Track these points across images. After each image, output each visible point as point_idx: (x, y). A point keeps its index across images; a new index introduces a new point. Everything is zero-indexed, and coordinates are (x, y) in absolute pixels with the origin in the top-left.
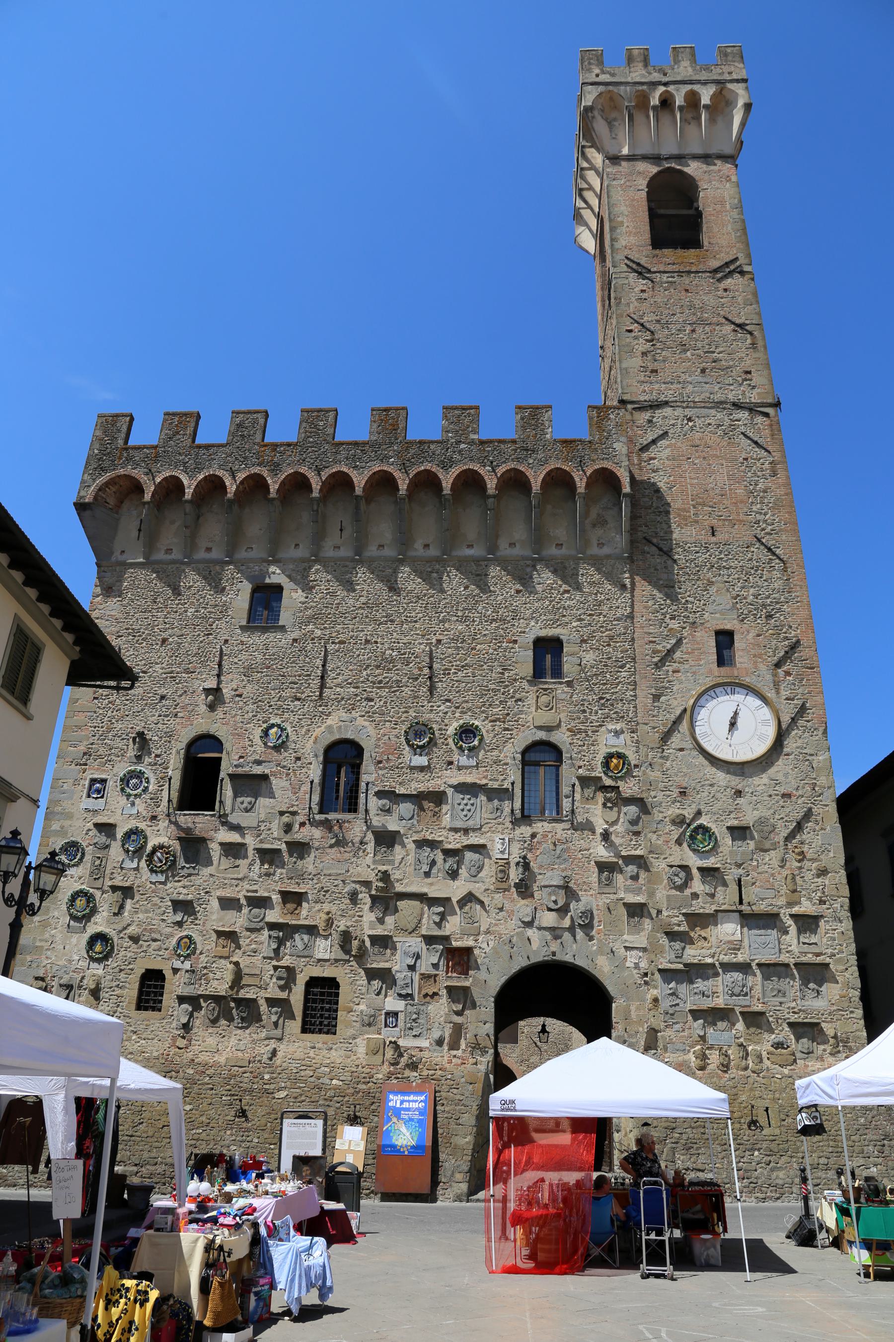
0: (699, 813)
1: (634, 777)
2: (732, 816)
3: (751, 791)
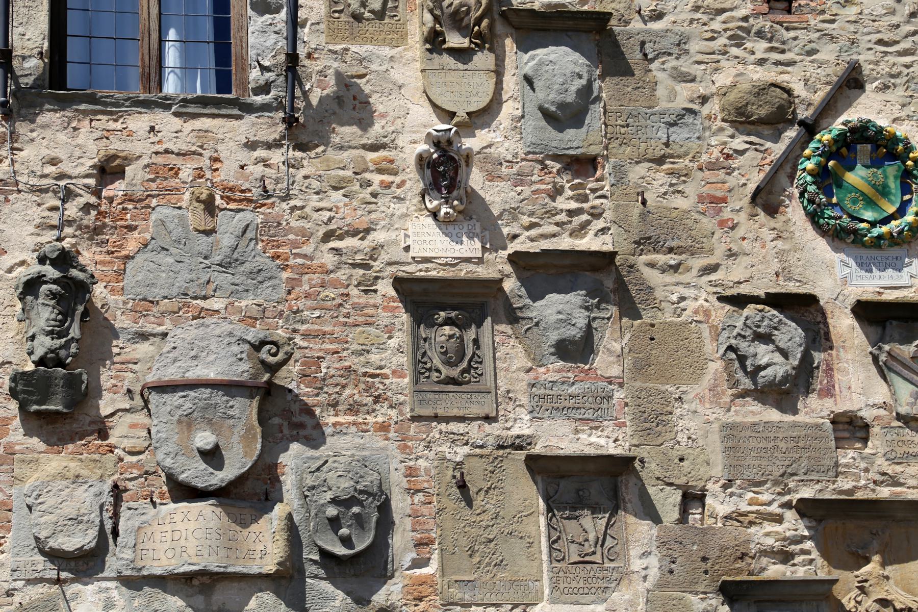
0: (852, 82)
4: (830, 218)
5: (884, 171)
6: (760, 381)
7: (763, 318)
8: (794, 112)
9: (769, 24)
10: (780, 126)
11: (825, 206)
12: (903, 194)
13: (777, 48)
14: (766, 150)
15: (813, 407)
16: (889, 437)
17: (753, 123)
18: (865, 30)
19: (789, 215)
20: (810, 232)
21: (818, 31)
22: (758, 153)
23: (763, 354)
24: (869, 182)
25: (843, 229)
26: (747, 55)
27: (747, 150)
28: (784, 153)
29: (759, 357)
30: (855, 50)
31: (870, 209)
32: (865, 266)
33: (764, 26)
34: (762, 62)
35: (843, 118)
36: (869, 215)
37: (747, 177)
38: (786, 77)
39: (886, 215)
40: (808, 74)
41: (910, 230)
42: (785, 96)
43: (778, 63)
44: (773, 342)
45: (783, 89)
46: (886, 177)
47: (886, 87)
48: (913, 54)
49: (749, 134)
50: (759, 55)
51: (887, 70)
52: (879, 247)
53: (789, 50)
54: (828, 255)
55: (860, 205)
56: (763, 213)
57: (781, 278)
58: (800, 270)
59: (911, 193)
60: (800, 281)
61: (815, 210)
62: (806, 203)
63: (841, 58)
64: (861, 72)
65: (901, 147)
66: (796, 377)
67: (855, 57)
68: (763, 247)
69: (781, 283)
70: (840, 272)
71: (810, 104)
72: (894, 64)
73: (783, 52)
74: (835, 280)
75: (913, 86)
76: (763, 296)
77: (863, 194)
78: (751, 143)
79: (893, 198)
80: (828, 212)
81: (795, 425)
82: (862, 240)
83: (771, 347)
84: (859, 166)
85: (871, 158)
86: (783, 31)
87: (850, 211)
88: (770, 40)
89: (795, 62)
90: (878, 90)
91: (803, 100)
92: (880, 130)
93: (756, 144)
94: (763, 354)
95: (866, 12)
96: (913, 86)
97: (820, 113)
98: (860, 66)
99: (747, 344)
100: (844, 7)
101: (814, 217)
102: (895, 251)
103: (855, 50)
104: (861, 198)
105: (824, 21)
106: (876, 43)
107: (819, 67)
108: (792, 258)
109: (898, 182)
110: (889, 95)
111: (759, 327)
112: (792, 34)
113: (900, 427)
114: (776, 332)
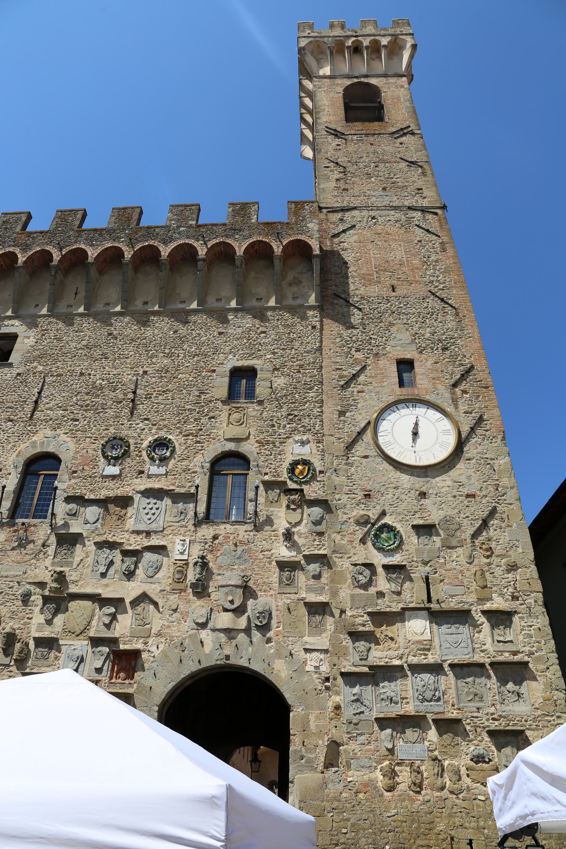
1: (318, 481)
2: (417, 515)
3: (435, 492)
34: (363, 510)
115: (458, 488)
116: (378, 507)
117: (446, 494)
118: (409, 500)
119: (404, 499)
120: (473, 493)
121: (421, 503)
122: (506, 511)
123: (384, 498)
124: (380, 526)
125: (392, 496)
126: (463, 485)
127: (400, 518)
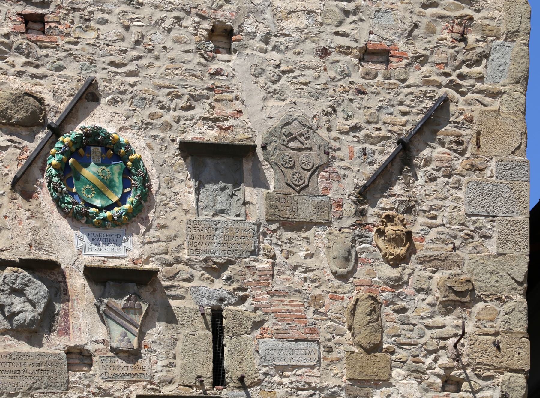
0: (89, 95)
2: (200, 111)
3: (263, 30)
4: (69, 203)
5: (112, 168)
6: (15, 323)
7: (17, 277)
8: (45, 118)
9: (26, 42)
10: (35, 128)
11: (66, 193)
12: (124, 187)
13: (33, 63)
14: (23, 147)
15: (54, 342)
16: (104, 363)
17: (12, 125)
18: (101, 53)
19: (40, 200)
20: (56, 214)
21: (65, 50)
22: (17, 150)
23: (18, 303)
24: (99, 177)
25: (78, 212)
26: (8, 67)
27: (8, 147)
28: (36, 150)
29: (14, 306)
30: (93, 69)
31: (99, 198)
32: (95, 241)
33: (22, 43)
34: (20, 74)
35: (83, 124)
36: (98, 202)
37: (9, 168)
38: (38, 88)
39: (111, 202)
40: (56, 87)
41: (127, 214)
42: (37, 104)
43: (33, 76)
44: (25, 295)
45: (35, 98)
46: (112, 174)
47: (115, 102)
48: (136, 75)
49: (10, 134)
50: (18, 68)
51: (117, 87)
52: (105, 227)
53: (42, 65)
54: (68, 232)
55: (93, 194)
56: (20, 198)
57: (33, 248)
58: (48, 242)
59: (131, 187)
60: (47, 251)
61: (58, 196)
62: (52, 190)
63: (82, 75)
64: (97, 88)
65: (123, 150)
66: (42, 320)
67: (93, 75)
68: (20, 224)
69: (34, 251)
70: (77, 245)
71: (57, 112)
72: (122, 83)
73: (37, 66)
74: (73, 251)
75: (136, 102)
76: (18, 261)
77: (94, 186)
78: (11, 141)
79: (117, 190)
80: (68, 199)
81: (40, 355)
82: (92, 221)
83: (23, 299)
84: (92, 164)
85: (102, 158)
86: (38, 49)
87: (85, 198)
88: (28, 56)
89: (47, 76)
90: (110, 103)
91: (52, 108)
92: (108, 136)
93: (16, 142)
94: (18, 303)
95: (102, 37)
96: (136, 102)
97: (64, 119)
98: (96, 83)
99: (5, 296)
100: (85, 31)
101: (58, 202)
102: (117, 231)
103: (93, 69)
104: (93, 189)
105: (69, 43)
106: (109, 64)
107: (65, 81)
108: (42, 233)
109: (121, 177)
110: (118, 109)
111: (14, 284)
112: (44, 52)
113: (112, 356)
114: (27, 288)
115: (340, 23)
116: (72, 70)
117: (298, 42)
118: (176, 52)
119: (159, 47)
120: (386, 45)
121: (214, 67)
122: (476, 115)
123: (91, 36)
124: (79, 138)
125: (121, 30)
126: (355, 12)
127: (144, 114)
